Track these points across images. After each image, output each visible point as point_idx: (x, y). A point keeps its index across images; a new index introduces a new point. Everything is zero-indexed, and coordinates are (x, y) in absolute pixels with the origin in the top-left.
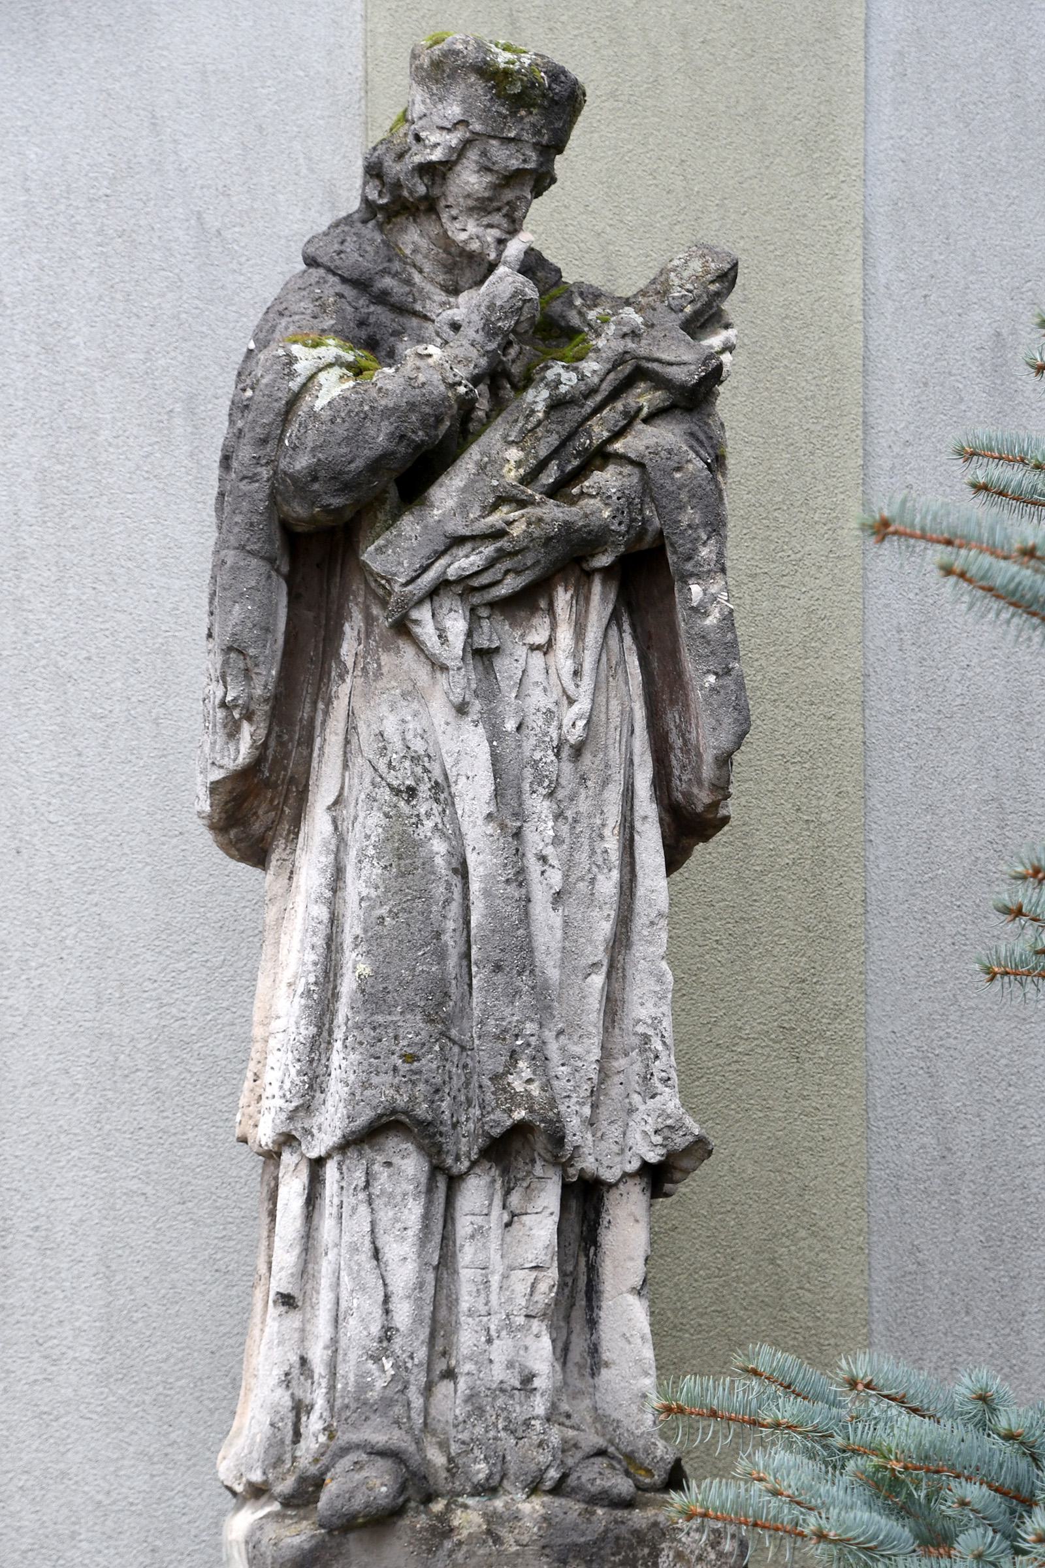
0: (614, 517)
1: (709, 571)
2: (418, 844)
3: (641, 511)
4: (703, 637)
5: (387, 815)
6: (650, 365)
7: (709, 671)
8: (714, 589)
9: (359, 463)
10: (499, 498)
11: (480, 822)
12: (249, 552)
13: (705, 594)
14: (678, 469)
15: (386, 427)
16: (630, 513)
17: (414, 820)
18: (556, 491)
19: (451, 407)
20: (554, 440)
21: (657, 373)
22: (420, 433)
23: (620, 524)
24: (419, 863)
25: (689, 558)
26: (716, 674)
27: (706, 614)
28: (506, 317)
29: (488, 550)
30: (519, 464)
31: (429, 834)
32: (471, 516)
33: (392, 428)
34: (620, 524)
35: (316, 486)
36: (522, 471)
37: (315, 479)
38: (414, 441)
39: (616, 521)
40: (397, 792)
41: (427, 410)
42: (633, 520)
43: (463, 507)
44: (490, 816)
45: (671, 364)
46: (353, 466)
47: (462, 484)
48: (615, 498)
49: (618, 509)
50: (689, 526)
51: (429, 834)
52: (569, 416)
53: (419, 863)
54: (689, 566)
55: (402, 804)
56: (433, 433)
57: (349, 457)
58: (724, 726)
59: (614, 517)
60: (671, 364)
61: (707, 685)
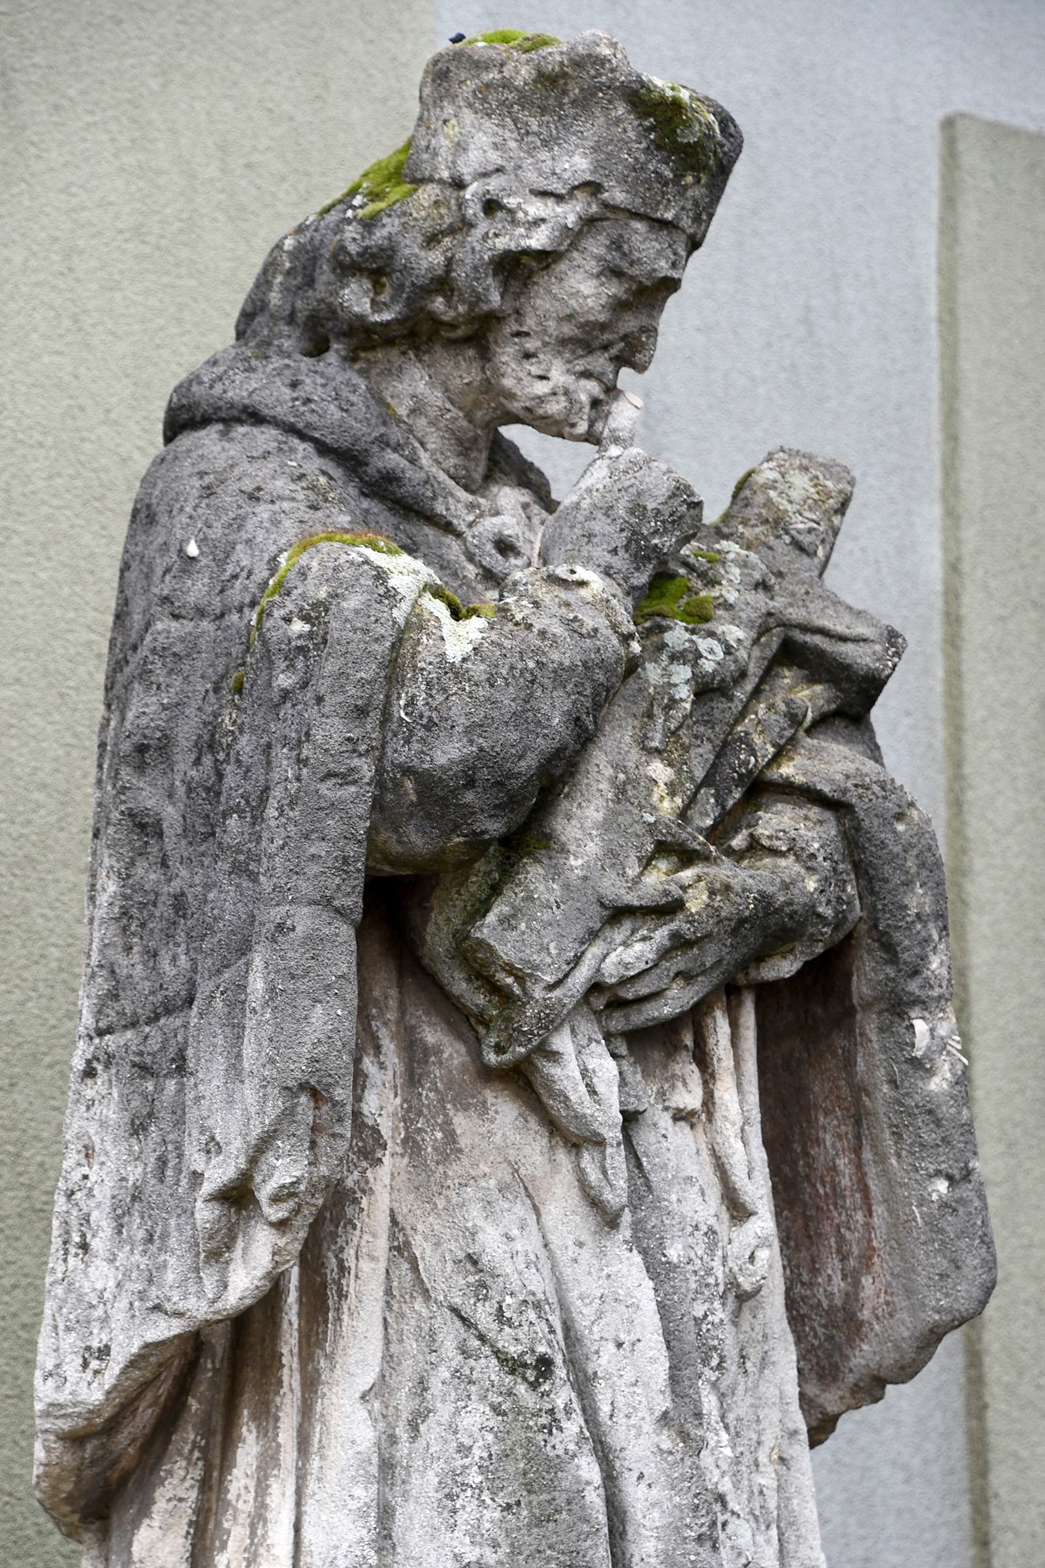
1: (940, 997)
2: (556, 1466)
4: (930, 1112)
5: (497, 1410)
6: (808, 638)
7: (938, 1173)
8: (942, 1031)
11: (648, 1427)
12: (337, 910)
13: (933, 1037)
14: (900, 817)
17: (544, 1420)
21: (821, 654)
24: (561, 1500)
25: (916, 973)
26: (950, 1178)
27: (931, 1073)
29: (661, 935)
31: (572, 1447)
35: (469, 797)
37: (471, 783)
40: (512, 1365)
43: (612, 855)
44: (665, 1419)
45: (844, 639)
50: (918, 915)
51: (572, 1447)
53: (561, 1500)
54: (913, 986)
55: (522, 1389)
58: (966, 1270)
60: (844, 639)
61: (935, 1197)
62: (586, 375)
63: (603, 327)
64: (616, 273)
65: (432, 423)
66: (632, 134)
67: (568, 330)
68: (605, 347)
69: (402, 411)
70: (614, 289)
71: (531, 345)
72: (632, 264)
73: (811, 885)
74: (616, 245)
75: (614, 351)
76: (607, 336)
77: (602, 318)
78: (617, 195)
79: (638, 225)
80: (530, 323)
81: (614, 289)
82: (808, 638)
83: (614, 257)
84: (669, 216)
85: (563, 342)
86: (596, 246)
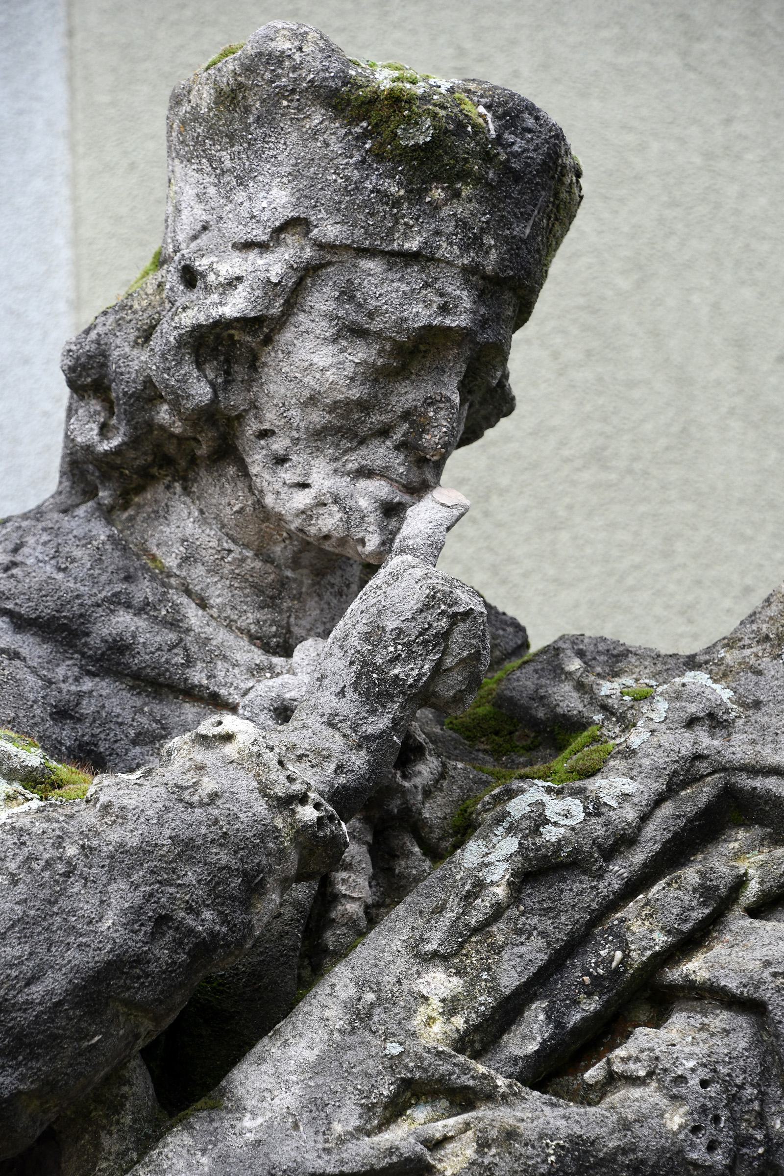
0: (696, 1130)
3: (761, 1119)
9: (54, 983)
10: (406, 1084)
15: (122, 896)
16: (733, 1120)
18: (550, 1072)
19: (282, 853)
20: (535, 951)
22: (207, 914)
23: (711, 1147)
28: (411, 656)
30: (451, 1006)
32: (338, 1128)
33: (137, 898)
34: (711, 1147)
36: (459, 1022)
38: (191, 931)
39: (701, 1141)
41: (224, 857)
42: (742, 1141)
43: (317, 1108)
46: (37, 990)
47: (311, 1056)
48: (694, 1081)
49: (704, 1110)
56: (239, 917)
57: (28, 968)
59: (696, 1130)
63: (364, 406)
64: (357, 332)
67: (317, 417)
68: (384, 432)
70: (361, 353)
71: (279, 445)
72: (371, 315)
73: (675, 1120)
74: (347, 294)
76: (377, 419)
77: (355, 393)
78: (330, 230)
80: (271, 418)
81: (361, 353)
82: (758, 783)
84: (413, 245)
86: (321, 300)
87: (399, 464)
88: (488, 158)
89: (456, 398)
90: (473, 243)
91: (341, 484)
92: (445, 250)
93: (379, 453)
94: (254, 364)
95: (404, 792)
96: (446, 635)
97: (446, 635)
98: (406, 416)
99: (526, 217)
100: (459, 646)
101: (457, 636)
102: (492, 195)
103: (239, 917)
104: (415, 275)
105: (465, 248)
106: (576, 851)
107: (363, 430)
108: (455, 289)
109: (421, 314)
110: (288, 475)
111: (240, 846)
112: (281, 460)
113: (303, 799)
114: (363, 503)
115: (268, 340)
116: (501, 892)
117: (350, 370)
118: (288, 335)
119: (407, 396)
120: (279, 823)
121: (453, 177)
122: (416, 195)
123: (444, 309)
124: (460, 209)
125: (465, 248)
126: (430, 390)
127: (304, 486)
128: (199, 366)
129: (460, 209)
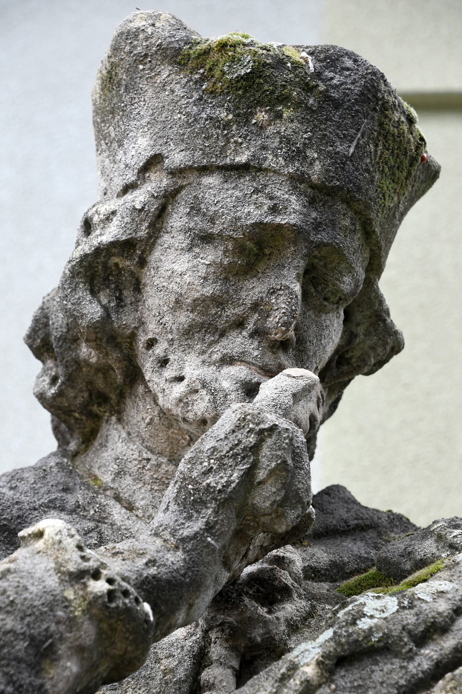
19: (71, 622)
28: (222, 467)
52: (377, 676)
56: (26, 678)
62: (228, 360)
63: (218, 302)
64: (206, 238)
65: (138, 479)
66: (179, 91)
67: (184, 318)
68: (239, 324)
69: (107, 478)
70: (211, 255)
71: (159, 350)
72: (212, 221)
74: (195, 209)
75: (250, 326)
76: (232, 312)
77: (209, 290)
78: (177, 157)
79: (212, 180)
80: (152, 328)
83: (199, 223)
84: (242, 158)
85: (188, 333)
86: (178, 219)
87: (253, 349)
88: (309, 89)
89: (297, 288)
90: (297, 155)
91: (208, 372)
92: (270, 161)
93: (237, 342)
94: (138, 287)
95: (266, 623)
96: (255, 449)
97: (255, 449)
98: (255, 307)
99: (348, 139)
100: (268, 458)
101: (265, 451)
102: (310, 116)
103: (26, 678)
104: (247, 184)
105: (290, 159)
106: (386, 636)
107: (221, 324)
108: (282, 192)
109: (254, 213)
110: (169, 372)
111: (29, 613)
112: (164, 362)
113: (96, 575)
114: (226, 385)
115: (143, 263)
116: (310, 671)
117: (202, 271)
118: (157, 254)
119: (254, 290)
120: (70, 594)
121: (275, 101)
122: (244, 118)
123: (274, 210)
124: (284, 128)
125: (290, 159)
126: (273, 282)
127: (181, 379)
128: (94, 293)
129: (284, 128)
